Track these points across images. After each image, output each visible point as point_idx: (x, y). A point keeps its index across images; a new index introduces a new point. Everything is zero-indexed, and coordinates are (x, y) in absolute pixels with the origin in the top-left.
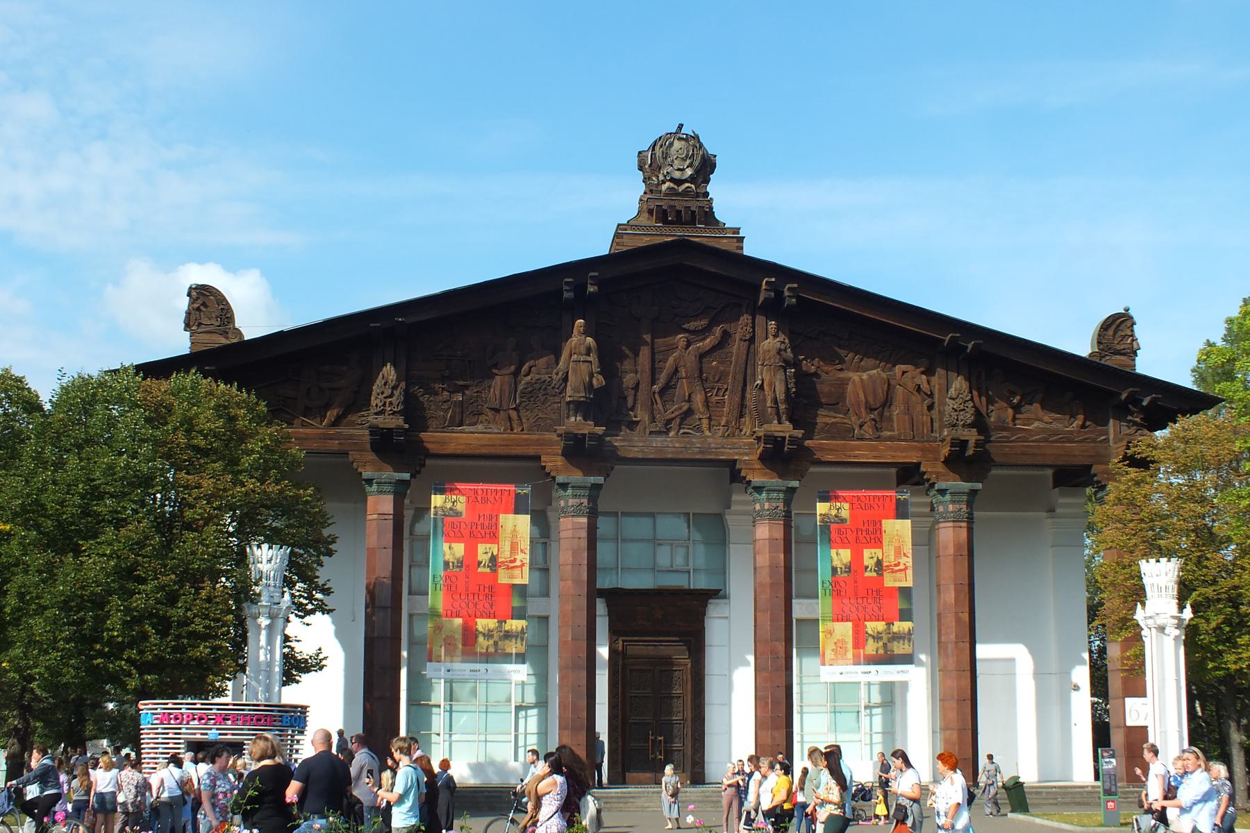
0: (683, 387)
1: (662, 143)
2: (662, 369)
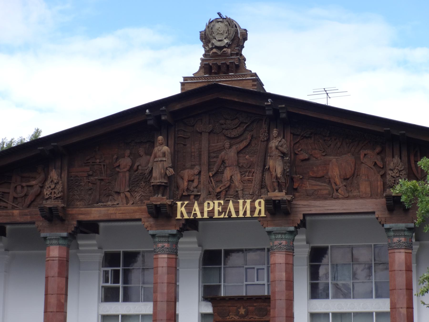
0: (227, 173)
2: (215, 162)
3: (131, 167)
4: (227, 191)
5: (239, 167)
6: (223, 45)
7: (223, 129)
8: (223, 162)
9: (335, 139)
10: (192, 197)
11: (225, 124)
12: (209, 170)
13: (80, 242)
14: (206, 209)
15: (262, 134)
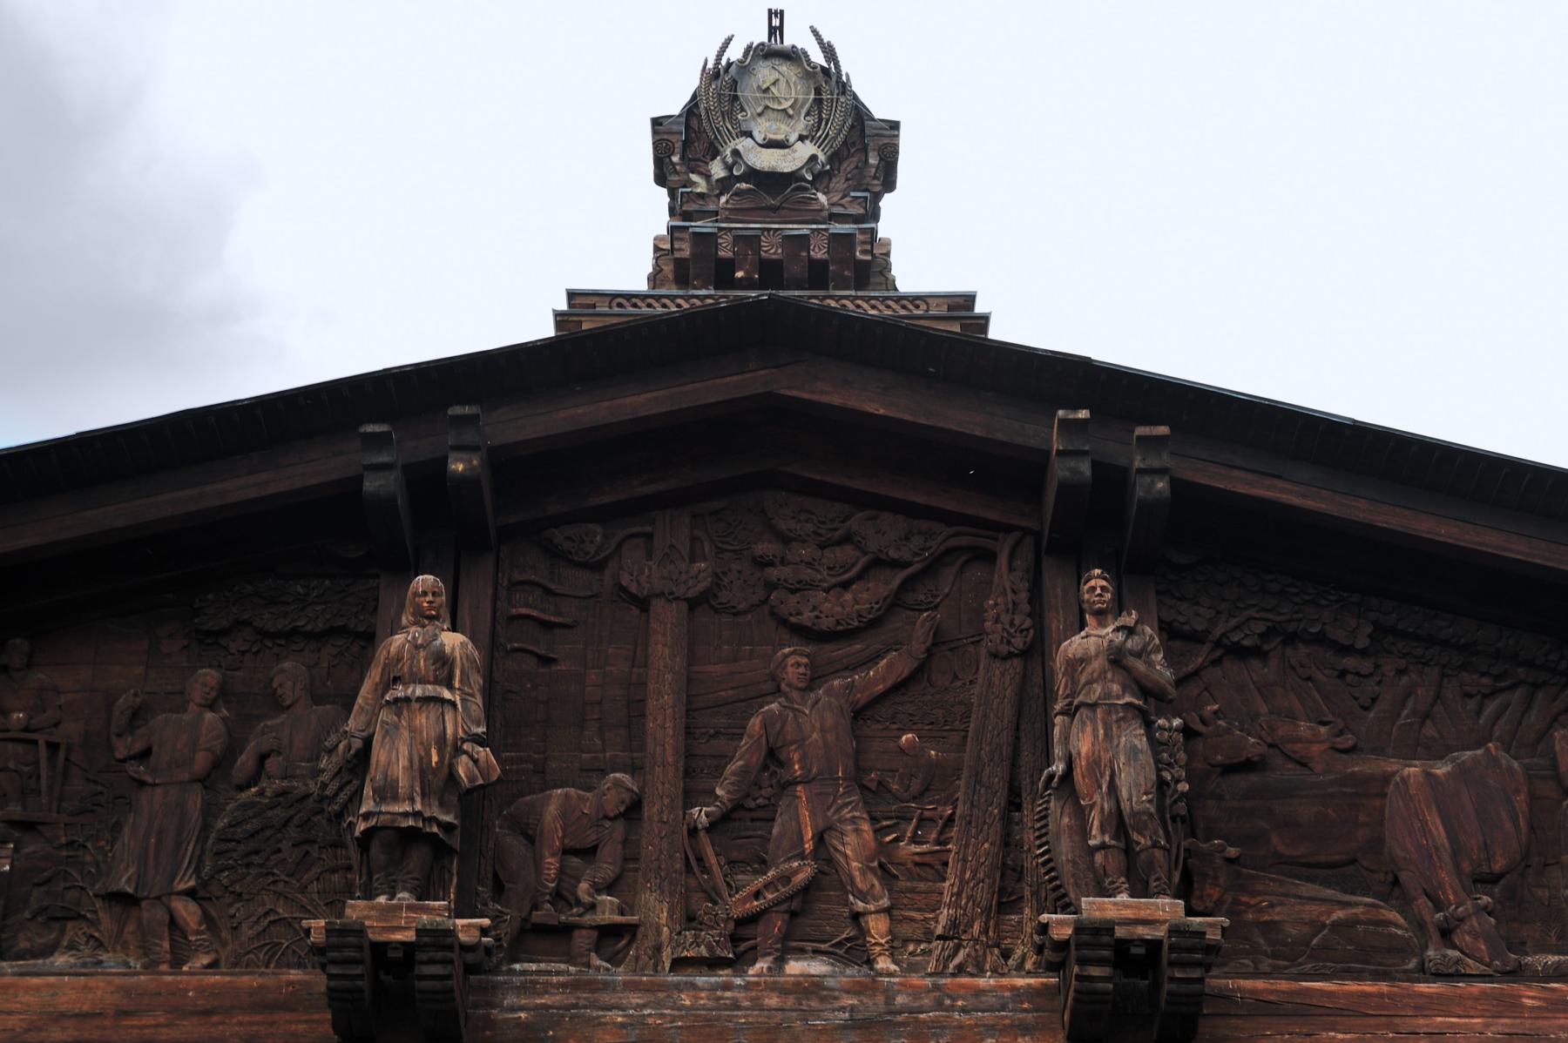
1: (724, 86)
3: (222, 762)
4: (793, 915)
5: (863, 787)
6: (787, 167)
7: (771, 586)
8: (773, 757)
9: (1401, 672)
10: (582, 940)
11: (784, 562)
15: (997, 621)
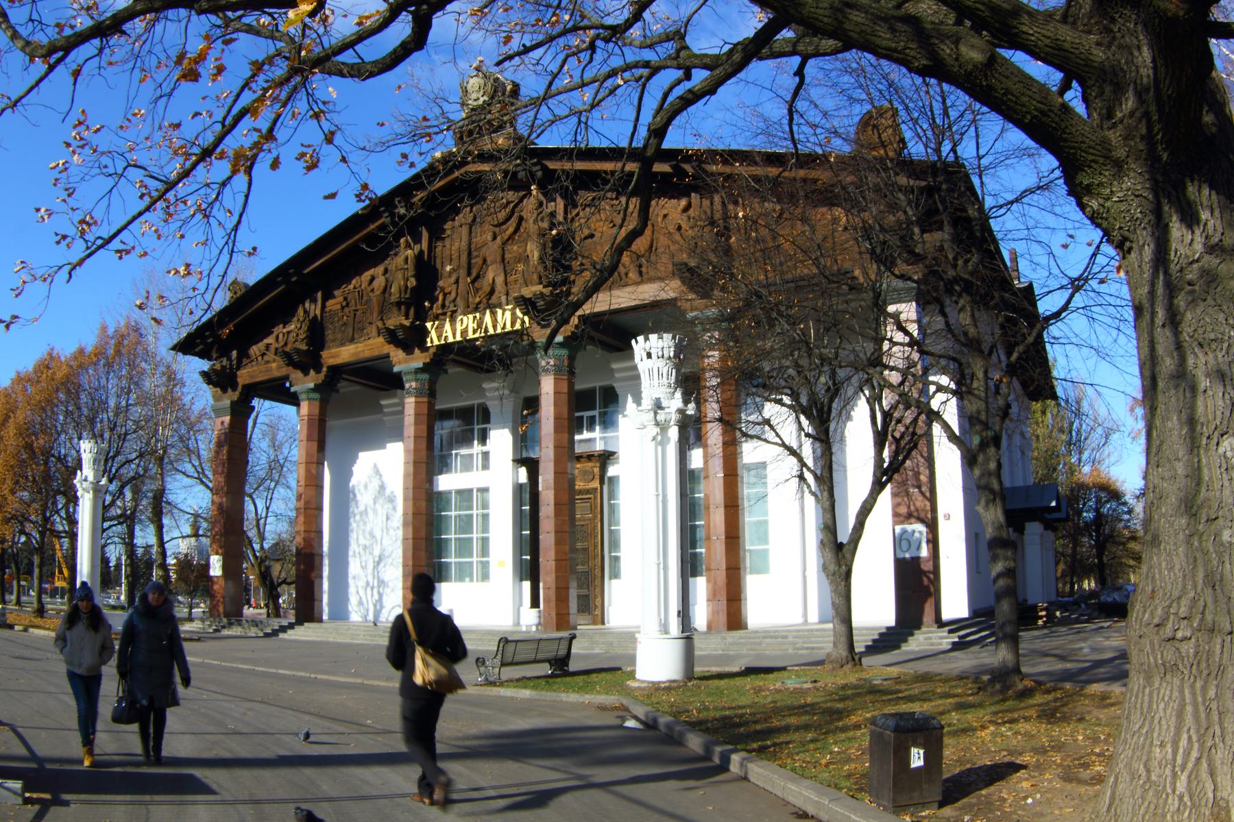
0: (490, 275)
8: (485, 260)
12: (469, 274)
13: (383, 402)
14: (459, 328)
